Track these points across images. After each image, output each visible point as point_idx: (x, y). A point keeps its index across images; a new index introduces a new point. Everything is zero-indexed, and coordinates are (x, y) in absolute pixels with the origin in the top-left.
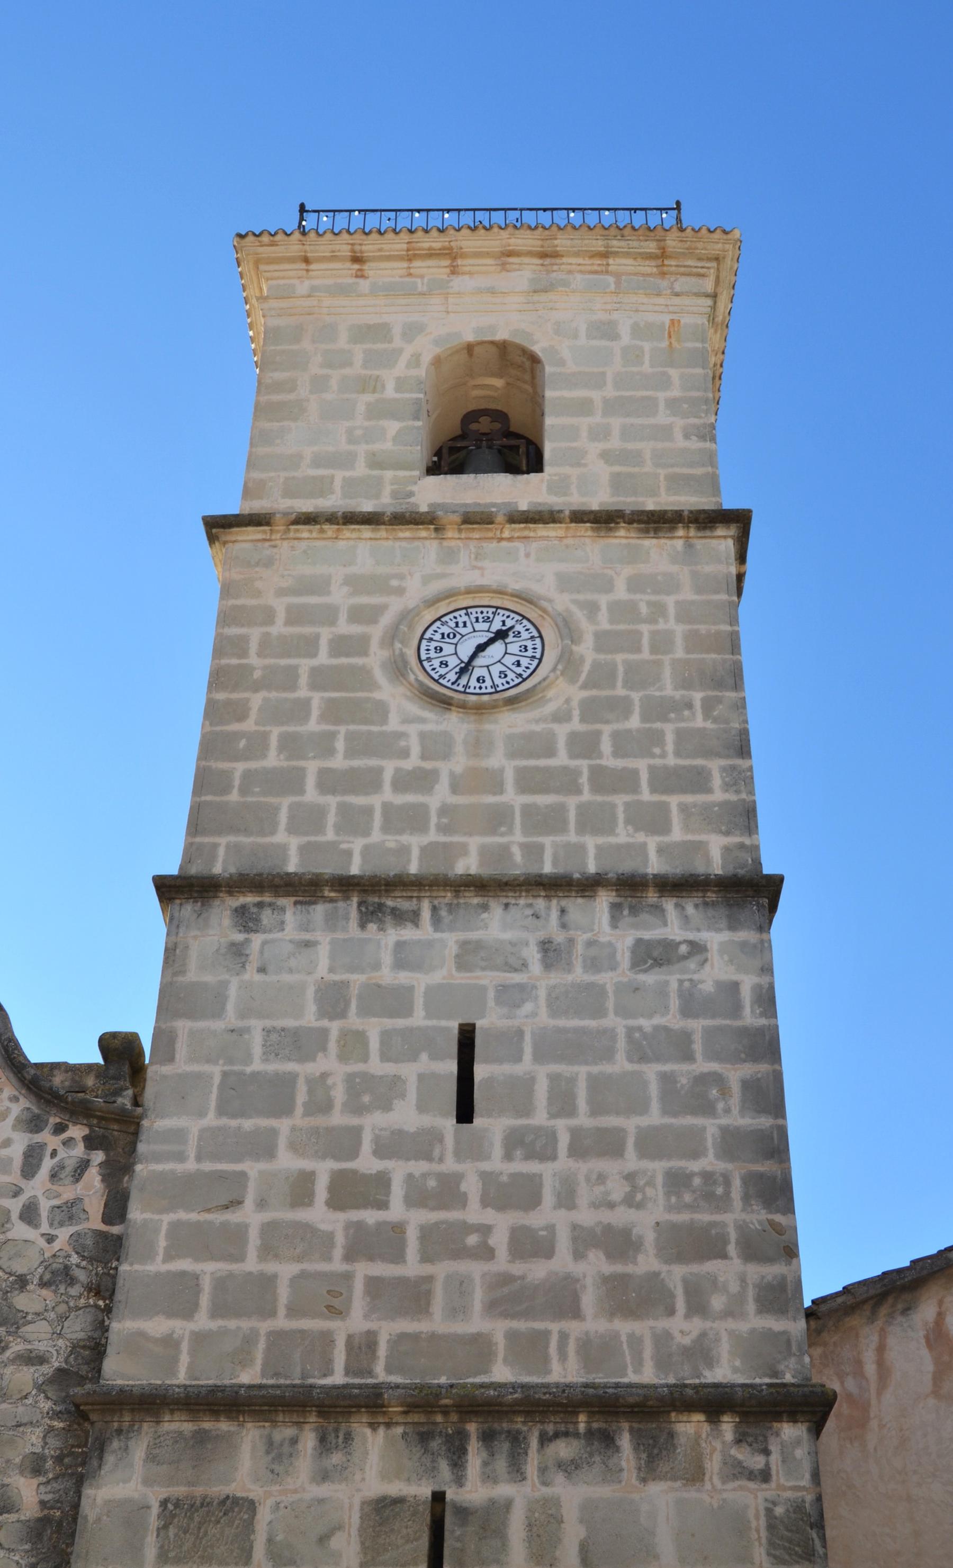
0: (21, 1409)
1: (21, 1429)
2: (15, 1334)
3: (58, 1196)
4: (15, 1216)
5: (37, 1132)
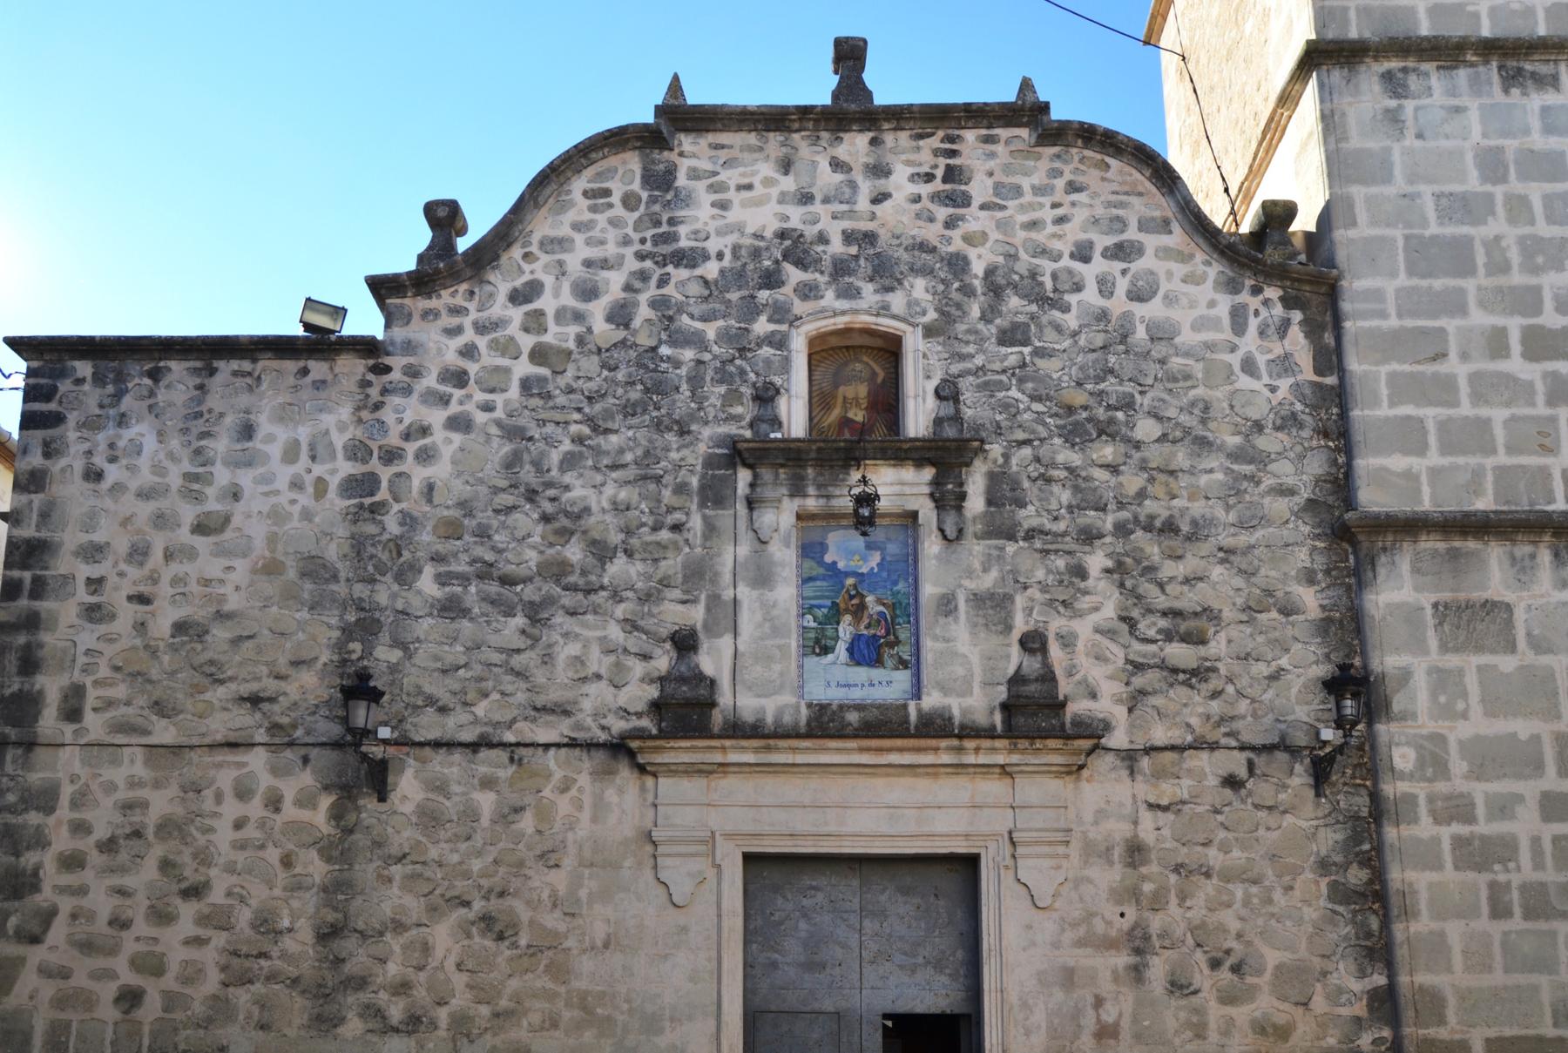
0: (1285, 532)
2: (1264, 470)
3: (1270, 351)
4: (1237, 368)
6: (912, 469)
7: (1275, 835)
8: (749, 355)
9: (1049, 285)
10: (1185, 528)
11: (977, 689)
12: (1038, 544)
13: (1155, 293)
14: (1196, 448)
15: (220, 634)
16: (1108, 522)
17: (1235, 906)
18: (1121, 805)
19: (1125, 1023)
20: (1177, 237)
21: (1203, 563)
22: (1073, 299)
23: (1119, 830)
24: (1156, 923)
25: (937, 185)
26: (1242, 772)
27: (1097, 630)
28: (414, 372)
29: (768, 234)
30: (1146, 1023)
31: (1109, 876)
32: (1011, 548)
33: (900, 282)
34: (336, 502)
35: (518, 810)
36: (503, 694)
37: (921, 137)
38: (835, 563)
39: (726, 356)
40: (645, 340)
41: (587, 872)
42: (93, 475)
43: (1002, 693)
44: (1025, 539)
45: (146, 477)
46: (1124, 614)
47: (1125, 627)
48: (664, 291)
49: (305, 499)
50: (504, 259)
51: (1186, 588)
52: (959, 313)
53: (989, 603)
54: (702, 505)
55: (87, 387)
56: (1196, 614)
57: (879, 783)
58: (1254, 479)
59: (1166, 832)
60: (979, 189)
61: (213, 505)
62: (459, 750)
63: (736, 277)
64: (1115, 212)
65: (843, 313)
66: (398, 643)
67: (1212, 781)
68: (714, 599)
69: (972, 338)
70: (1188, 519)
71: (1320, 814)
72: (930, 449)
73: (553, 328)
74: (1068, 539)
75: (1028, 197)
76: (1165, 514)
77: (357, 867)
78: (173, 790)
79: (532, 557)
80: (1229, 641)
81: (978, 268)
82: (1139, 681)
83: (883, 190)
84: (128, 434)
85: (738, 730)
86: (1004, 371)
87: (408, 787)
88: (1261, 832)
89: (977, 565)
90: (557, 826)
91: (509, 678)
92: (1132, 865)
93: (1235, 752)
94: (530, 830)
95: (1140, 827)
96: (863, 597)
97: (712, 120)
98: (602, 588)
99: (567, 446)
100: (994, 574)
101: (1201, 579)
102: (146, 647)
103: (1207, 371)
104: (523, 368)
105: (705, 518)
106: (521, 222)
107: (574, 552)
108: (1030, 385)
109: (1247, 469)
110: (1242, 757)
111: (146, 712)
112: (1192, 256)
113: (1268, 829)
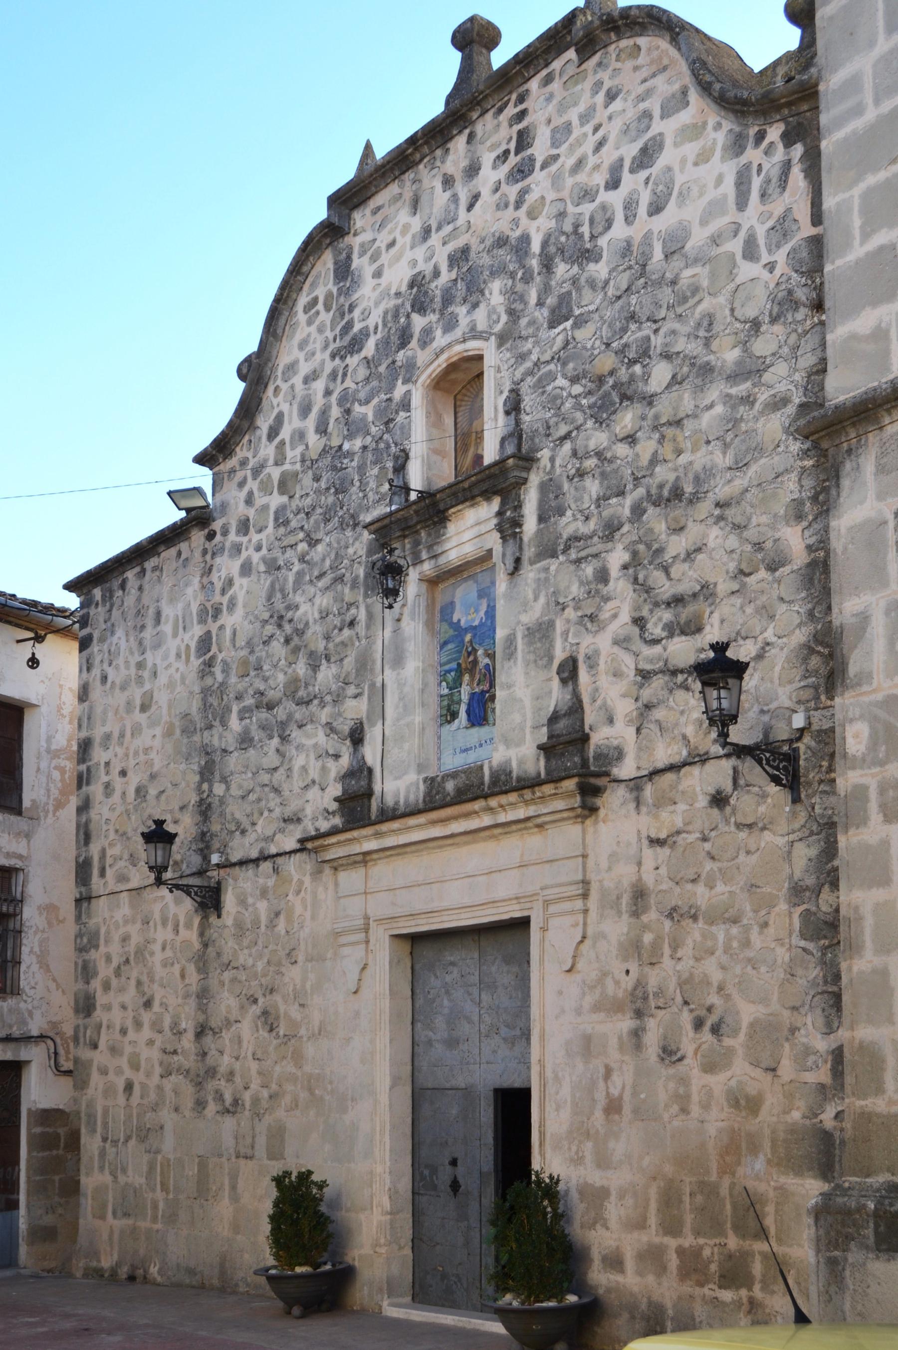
0: (777, 458)
1: (779, 479)
5: (742, 153)
6: (485, 504)
7: (754, 858)
8: (391, 426)
9: (587, 236)
10: (689, 489)
11: (528, 736)
12: (573, 555)
13: (670, 194)
14: (699, 381)
15: (153, 792)
16: (623, 507)
17: (718, 953)
18: (629, 844)
19: (627, 1097)
20: (697, 106)
21: (702, 527)
22: (603, 242)
23: (626, 873)
24: (653, 978)
25: (513, 160)
26: (728, 786)
27: (616, 642)
28: (225, 533)
29: (404, 288)
30: (643, 1096)
31: (616, 928)
32: (553, 565)
33: (482, 292)
34: (196, 663)
35: (277, 914)
36: (270, 811)
37: (501, 110)
38: (459, 621)
39: (379, 434)
40: (335, 442)
41: (310, 965)
42: (104, 679)
43: (543, 736)
44: (564, 552)
45: (123, 672)
46: (637, 615)
47: (637, 630)
48: (345, 385)
49: (181, 665)
50: (265, 403)
51: (686, 566)
52: (521, 307)
53: (538, 635)
54: (366, 596)
55: (100, 609)
56: (695, 595)
57: (464, 850)
58: (748, 400)
59: (663, 871)
60: (540, 149)
61: (147, 686)
62: (251, 866)
63: (384, 346)
64: (642, 106)
65: (442, 351)
66: (224, 780)
67: (702, 802)
68: (373, 685)
69: (531, 331)
70: (691, 476)
71: (797, 826)
72: (483, 480)
73: (290, 454)
74: (596, 539)
75: (576, 132)
76: (671, 477)
77: (210, 975)
78: (138, 925)
79: (281, 677)
80: (722, 621)
81: (536, 246)
82: (647, 694)
83: (475, 192)
84: (115, 639)
85: (389, 815)
86: (553, 358)
87: (229, 900)
88: (742, 857)
89: (531, 596)
90: (296, 925)
91: (272, 795)
92: (636, 914)
93: (724, 760)
94: (283, 932)
95: (643, 868)
96: (475, 651)
97: (366, 187)
98: (315, 697)
99: (297, 567)
100: (542, 600)
101: (698, 550)
102: (126, 811)
103: (713, 276)
104: (276, 500)
105: (368, 607)
106: (269, 360)
107: (301, 668)
108: (571, 365)
109: (743, 388)
110: (727, 765)
111: (127, 864)
112: (705, 123)
113: (748, 852)
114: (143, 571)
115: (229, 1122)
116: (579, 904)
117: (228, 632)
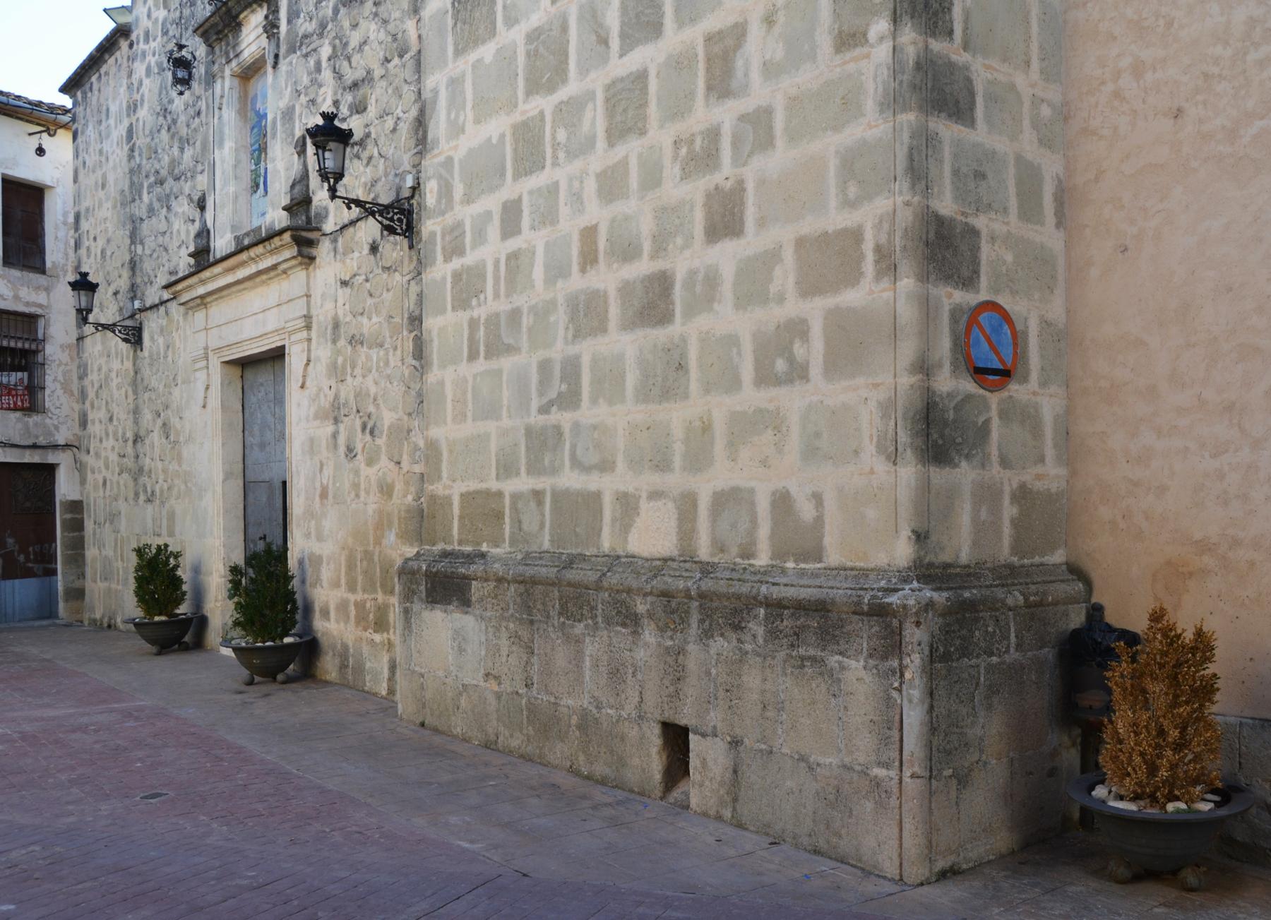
7: (391, 293)
59: (347, 307)
101: (365, 42)
114: (100, 76)
115: (150, 507)
116: (305, 334)
117: (141, 123)
